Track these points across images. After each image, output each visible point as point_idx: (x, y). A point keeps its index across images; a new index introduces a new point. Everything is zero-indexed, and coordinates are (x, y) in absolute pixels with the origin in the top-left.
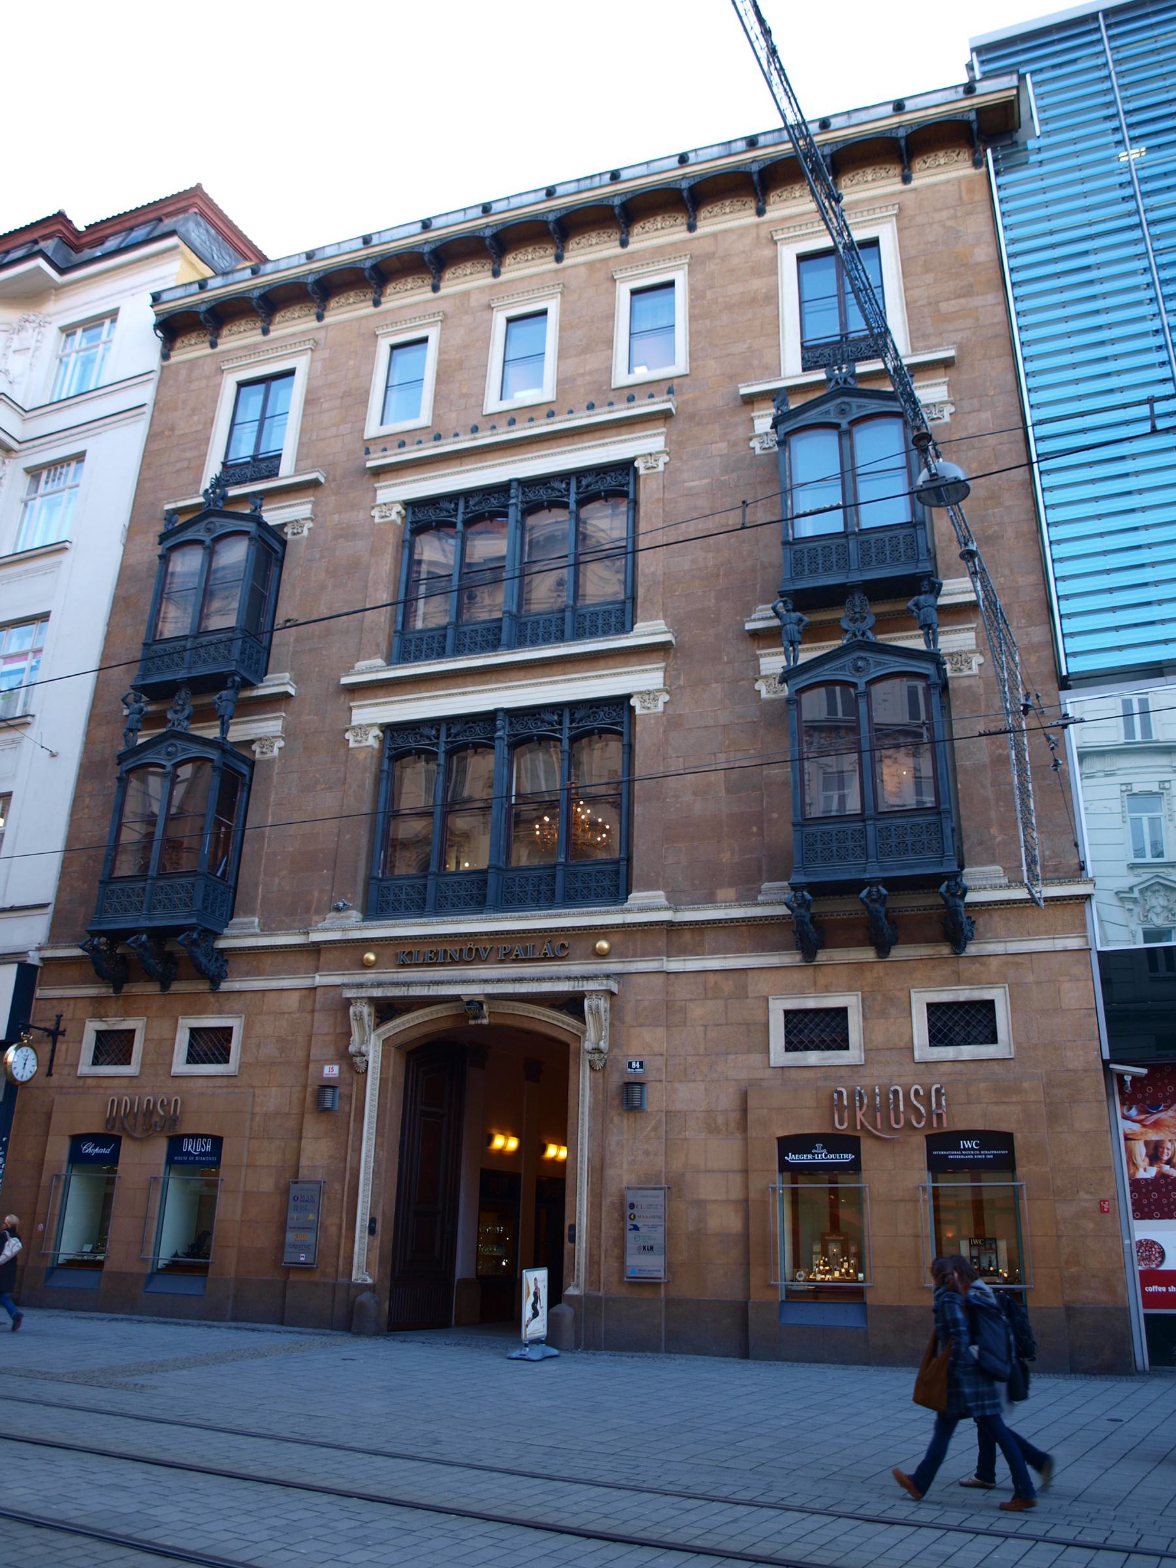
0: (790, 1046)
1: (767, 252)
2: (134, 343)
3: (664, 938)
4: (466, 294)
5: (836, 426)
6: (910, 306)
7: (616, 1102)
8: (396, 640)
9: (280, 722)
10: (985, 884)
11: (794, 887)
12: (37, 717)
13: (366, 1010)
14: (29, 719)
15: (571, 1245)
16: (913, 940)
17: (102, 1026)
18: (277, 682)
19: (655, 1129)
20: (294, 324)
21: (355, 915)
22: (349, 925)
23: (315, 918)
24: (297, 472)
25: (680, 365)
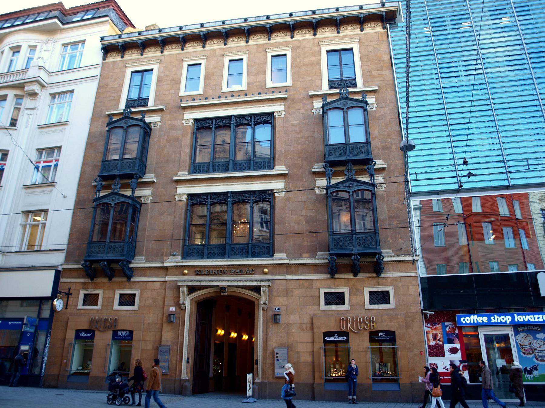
0: (326, 304)
1: (317, 48)
2: (92, 53)
4: (215, 50)
5: (342, 109)
6: (363, 71)
7: (271, 320)
8: (192, 166)
9: (151, 191)
10: (388, 255)
11: (330, 255)
12: (58, 183)
13: (186, 289)
14: (55, 184)
16: (365, 272)
17: (86, 292)
18: (149, 177)
19: (284, 329)
20: (152, 53)
21: (179, 258)
23: (165, 258)
24: (155, 105)
25: (289, 83)
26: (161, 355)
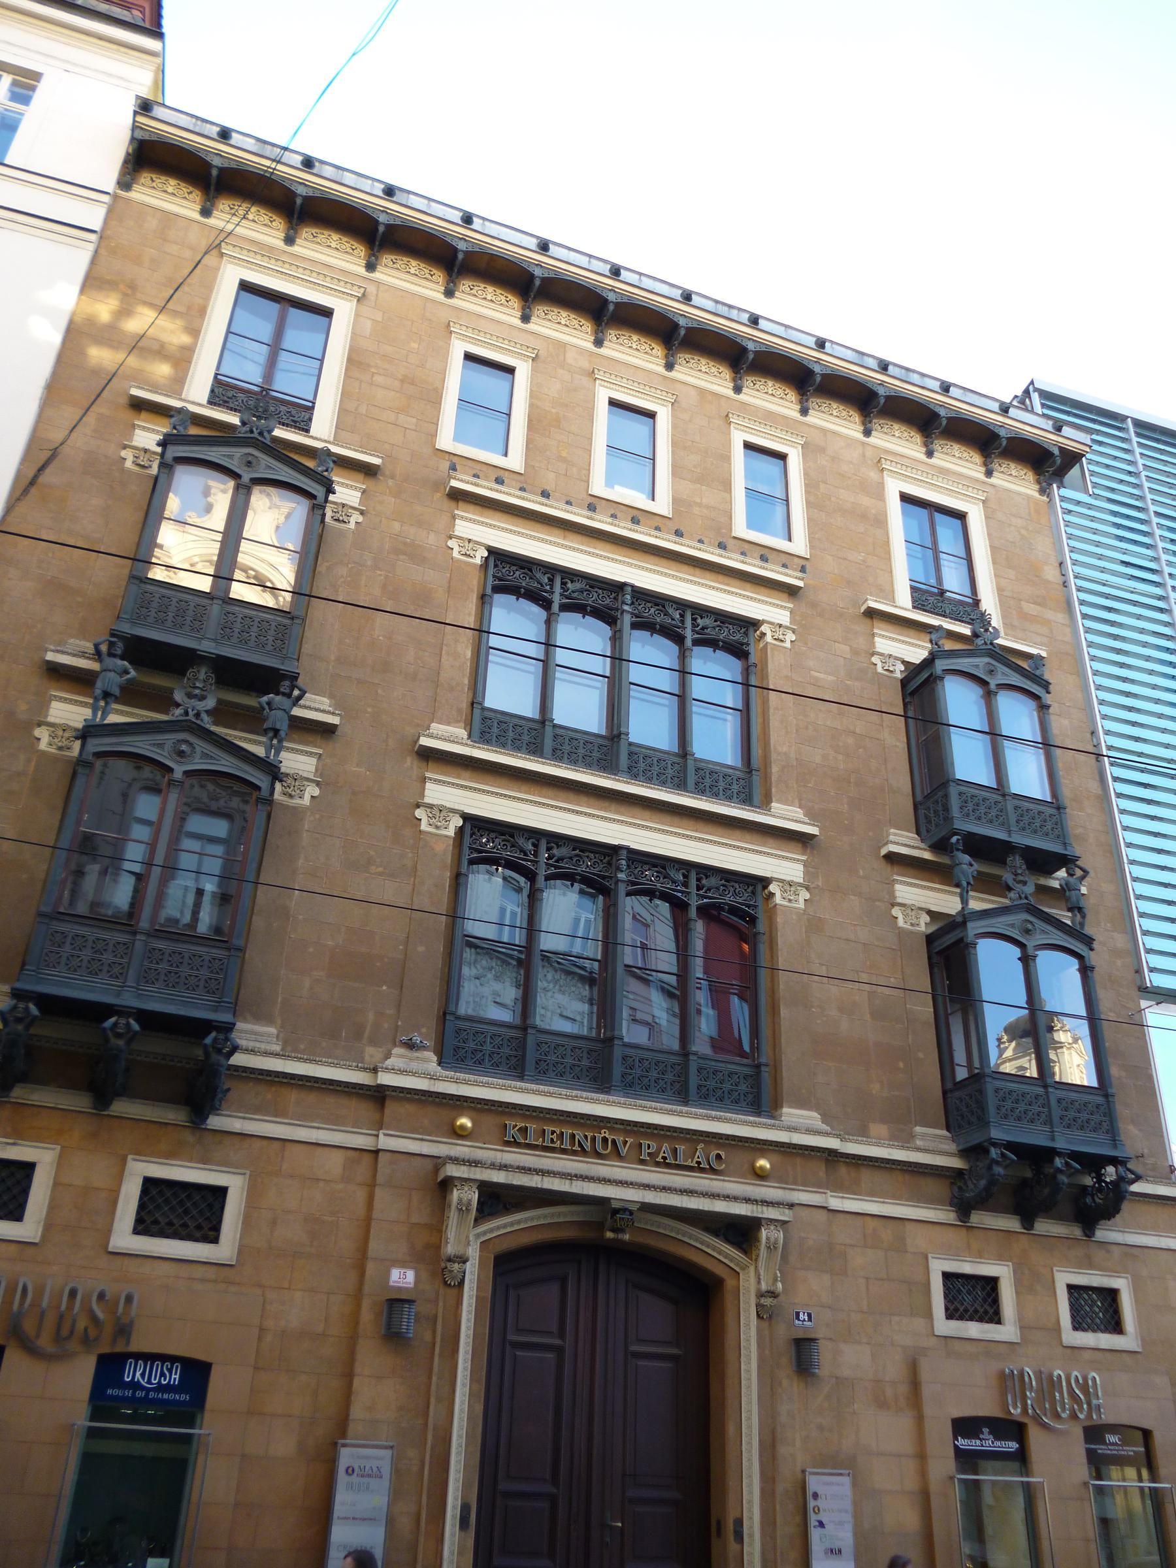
3: (824, 1168)
15: (737, 1547)
22: (413, 1070)
26: (350, 1487)
